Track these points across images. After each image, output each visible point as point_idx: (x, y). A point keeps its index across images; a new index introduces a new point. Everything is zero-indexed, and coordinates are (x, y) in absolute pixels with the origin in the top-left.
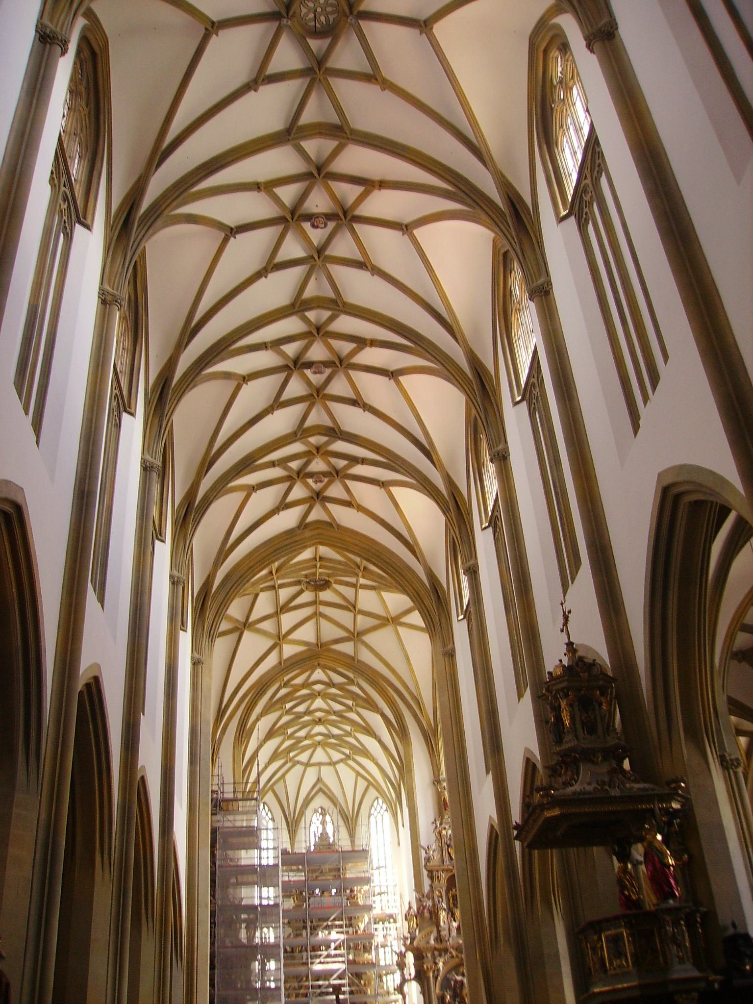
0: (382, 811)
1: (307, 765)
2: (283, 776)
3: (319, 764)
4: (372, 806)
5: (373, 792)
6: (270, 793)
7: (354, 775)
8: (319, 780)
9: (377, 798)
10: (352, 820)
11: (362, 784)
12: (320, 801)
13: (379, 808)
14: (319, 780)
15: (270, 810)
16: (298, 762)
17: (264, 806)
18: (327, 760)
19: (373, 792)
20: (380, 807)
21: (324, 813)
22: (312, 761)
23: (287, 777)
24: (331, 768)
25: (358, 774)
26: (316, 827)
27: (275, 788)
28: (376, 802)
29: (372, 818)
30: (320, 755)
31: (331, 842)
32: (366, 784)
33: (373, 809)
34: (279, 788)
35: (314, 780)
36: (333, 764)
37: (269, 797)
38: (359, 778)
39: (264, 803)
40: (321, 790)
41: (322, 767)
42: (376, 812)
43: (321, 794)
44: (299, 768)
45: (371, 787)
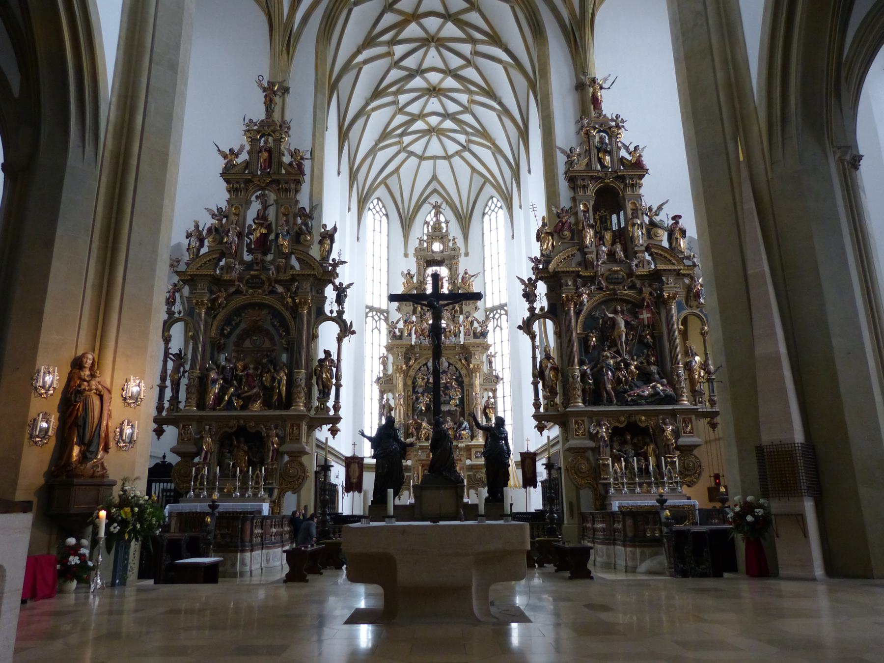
0: (496, 209)
1: (422, 158)
2: (397, 170)
3: (435, 158)
4: (486, 205)
5: (489, 190)
6: (383, 186)
7: (469, 170)
8: (434, 178)
9: (492, 197)
10: (465, 218)
11: (478, 181)
12: (434, 199)
13: (493, 206)
14: (434, 178)
15: (384, 206)
16: (412, 154)
17: (378, 202)
18: (443, 154)
19: (489, 190)
20: (497, 201)
21: (437, 207)
22: (427, 154)
23: (401, 170)
24: (446, 162)
25: (473, 169)
26: (431, 218)
27: (388, 181)
28: (491, 201)
29: (486, 217)
30: (435, 148)
31: (444, 231)
32: (483, 180)
33: (487, 208)
34: (393, 182)
35: (429, 177)
36: (448, 157)
37: (381, 191)
38: (475, 175)
39: (378, 199)
40: (435, 191)
41: (438, 161)
42: (490, 211)
43: (435, 194)
44: (413, 161)
45: (487, 184)
